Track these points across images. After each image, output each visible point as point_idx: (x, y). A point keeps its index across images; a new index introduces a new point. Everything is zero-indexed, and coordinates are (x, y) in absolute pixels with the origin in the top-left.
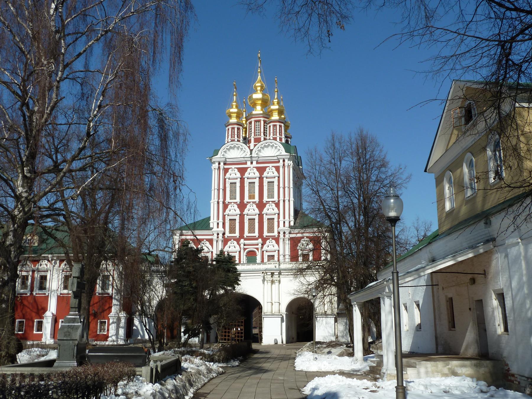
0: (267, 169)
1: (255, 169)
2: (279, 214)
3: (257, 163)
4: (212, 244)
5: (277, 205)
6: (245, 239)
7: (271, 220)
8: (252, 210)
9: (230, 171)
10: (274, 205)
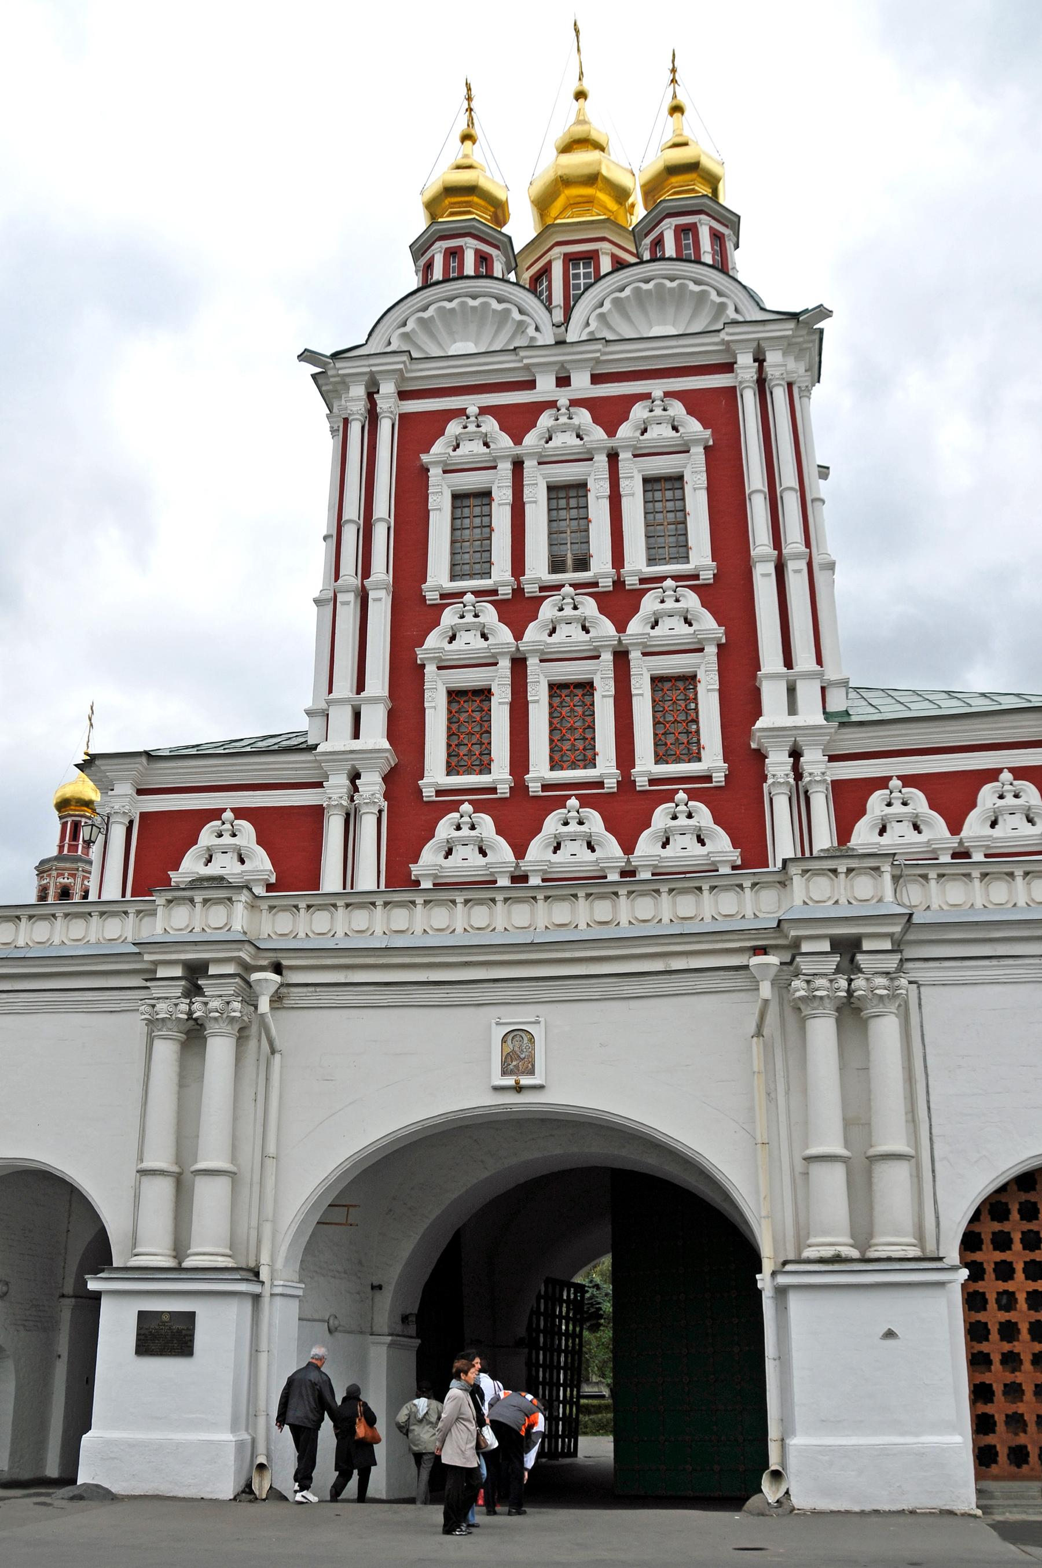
1: (583, 417)
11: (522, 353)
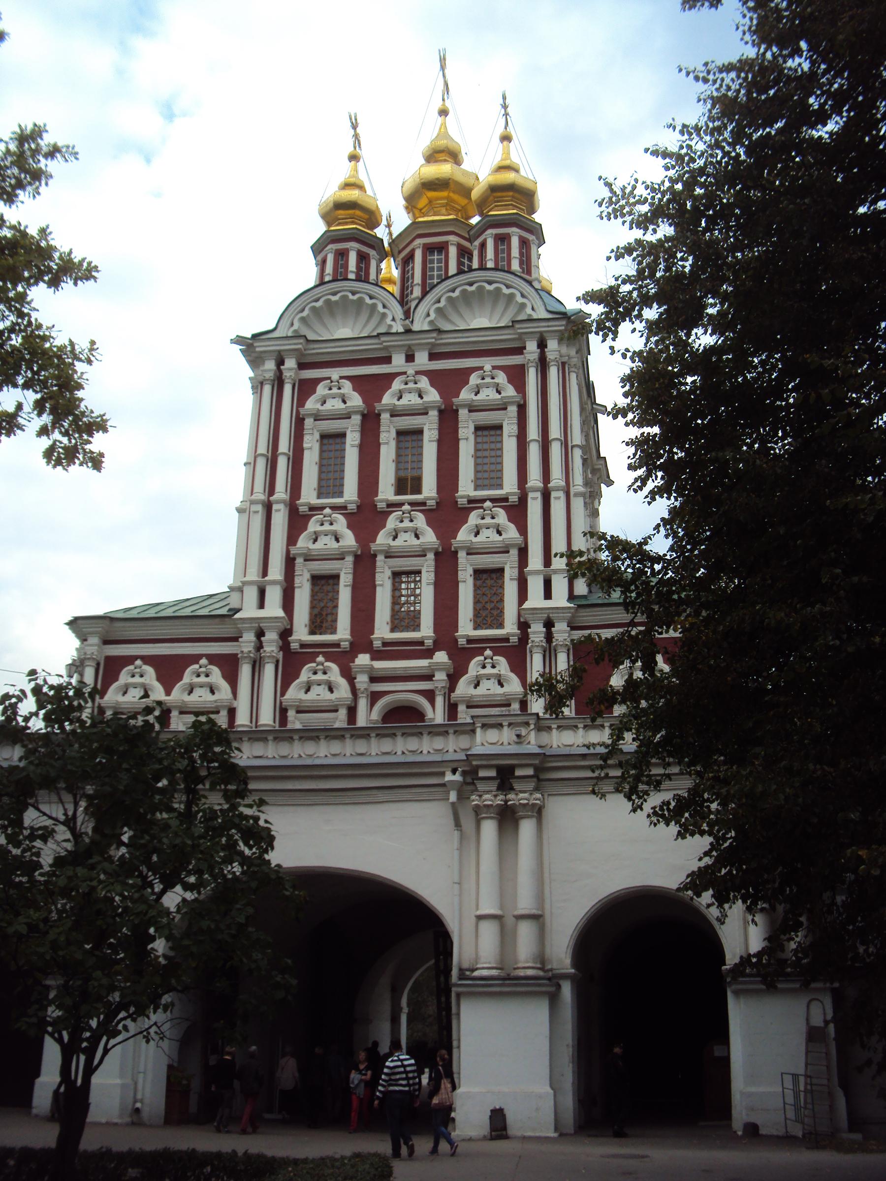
0: (474, 379)
1: (424, 383)
2: (523, 552)
3: (433, 357)
4: (232, 679)
5: (517, 512)
6: (377, 655)
7: (488, 578)
8: (408, 533)
9: (321, 390)
10: (502, 517)
11: (383, 339)
